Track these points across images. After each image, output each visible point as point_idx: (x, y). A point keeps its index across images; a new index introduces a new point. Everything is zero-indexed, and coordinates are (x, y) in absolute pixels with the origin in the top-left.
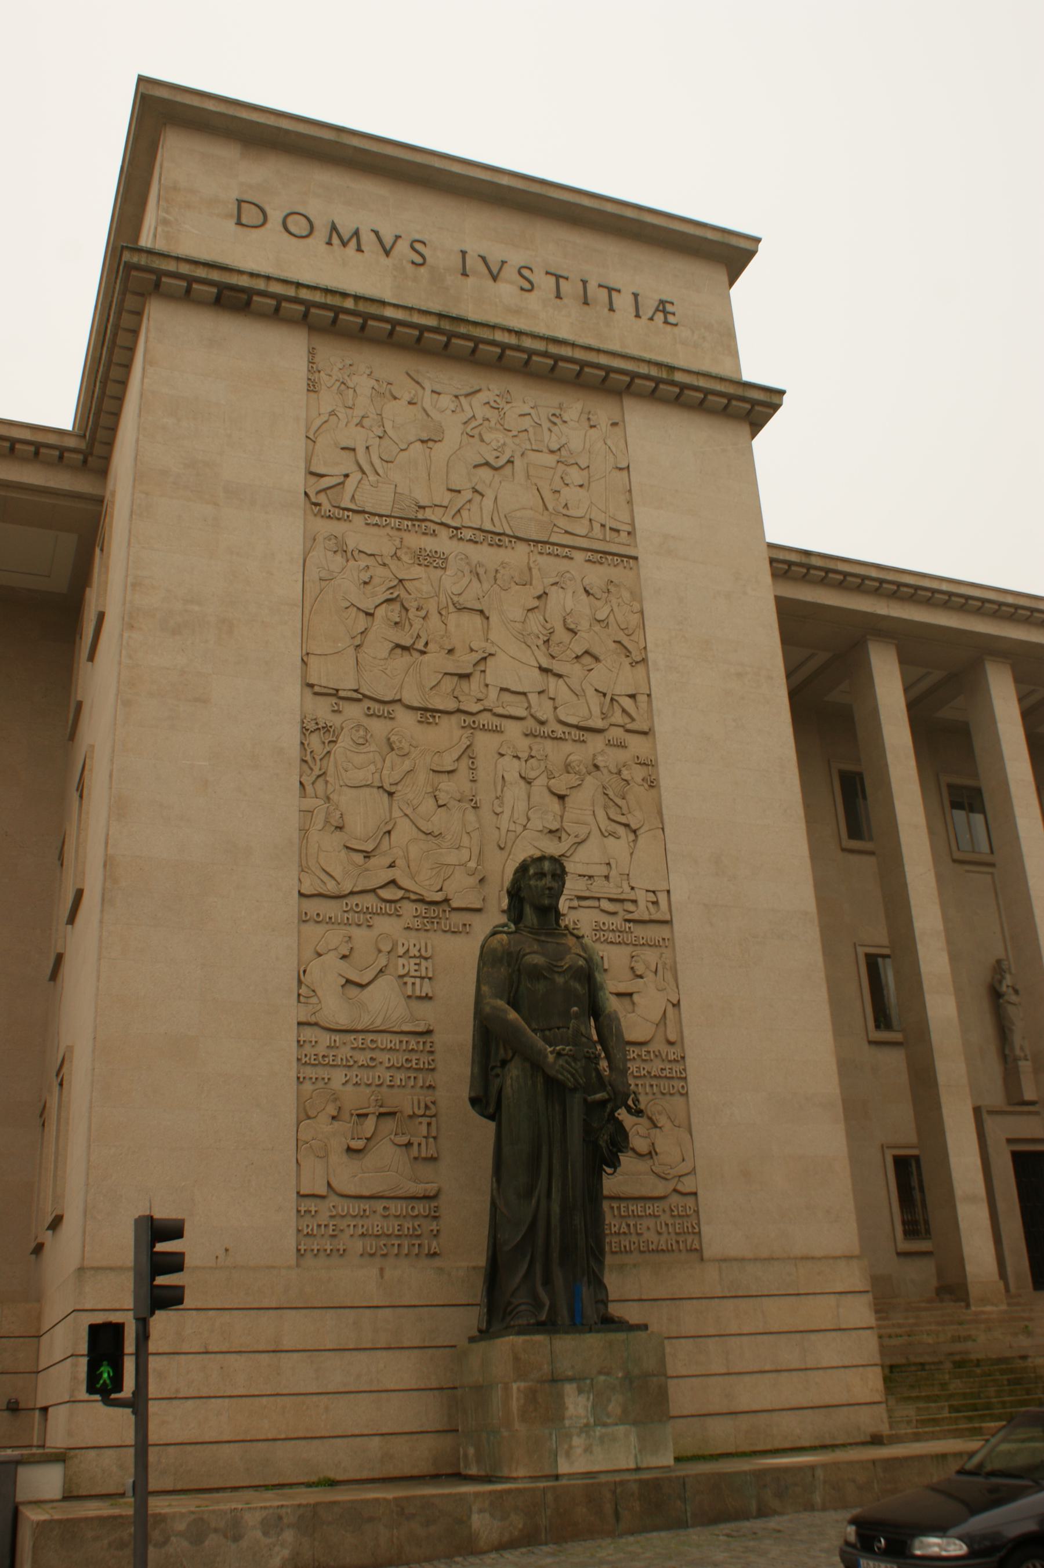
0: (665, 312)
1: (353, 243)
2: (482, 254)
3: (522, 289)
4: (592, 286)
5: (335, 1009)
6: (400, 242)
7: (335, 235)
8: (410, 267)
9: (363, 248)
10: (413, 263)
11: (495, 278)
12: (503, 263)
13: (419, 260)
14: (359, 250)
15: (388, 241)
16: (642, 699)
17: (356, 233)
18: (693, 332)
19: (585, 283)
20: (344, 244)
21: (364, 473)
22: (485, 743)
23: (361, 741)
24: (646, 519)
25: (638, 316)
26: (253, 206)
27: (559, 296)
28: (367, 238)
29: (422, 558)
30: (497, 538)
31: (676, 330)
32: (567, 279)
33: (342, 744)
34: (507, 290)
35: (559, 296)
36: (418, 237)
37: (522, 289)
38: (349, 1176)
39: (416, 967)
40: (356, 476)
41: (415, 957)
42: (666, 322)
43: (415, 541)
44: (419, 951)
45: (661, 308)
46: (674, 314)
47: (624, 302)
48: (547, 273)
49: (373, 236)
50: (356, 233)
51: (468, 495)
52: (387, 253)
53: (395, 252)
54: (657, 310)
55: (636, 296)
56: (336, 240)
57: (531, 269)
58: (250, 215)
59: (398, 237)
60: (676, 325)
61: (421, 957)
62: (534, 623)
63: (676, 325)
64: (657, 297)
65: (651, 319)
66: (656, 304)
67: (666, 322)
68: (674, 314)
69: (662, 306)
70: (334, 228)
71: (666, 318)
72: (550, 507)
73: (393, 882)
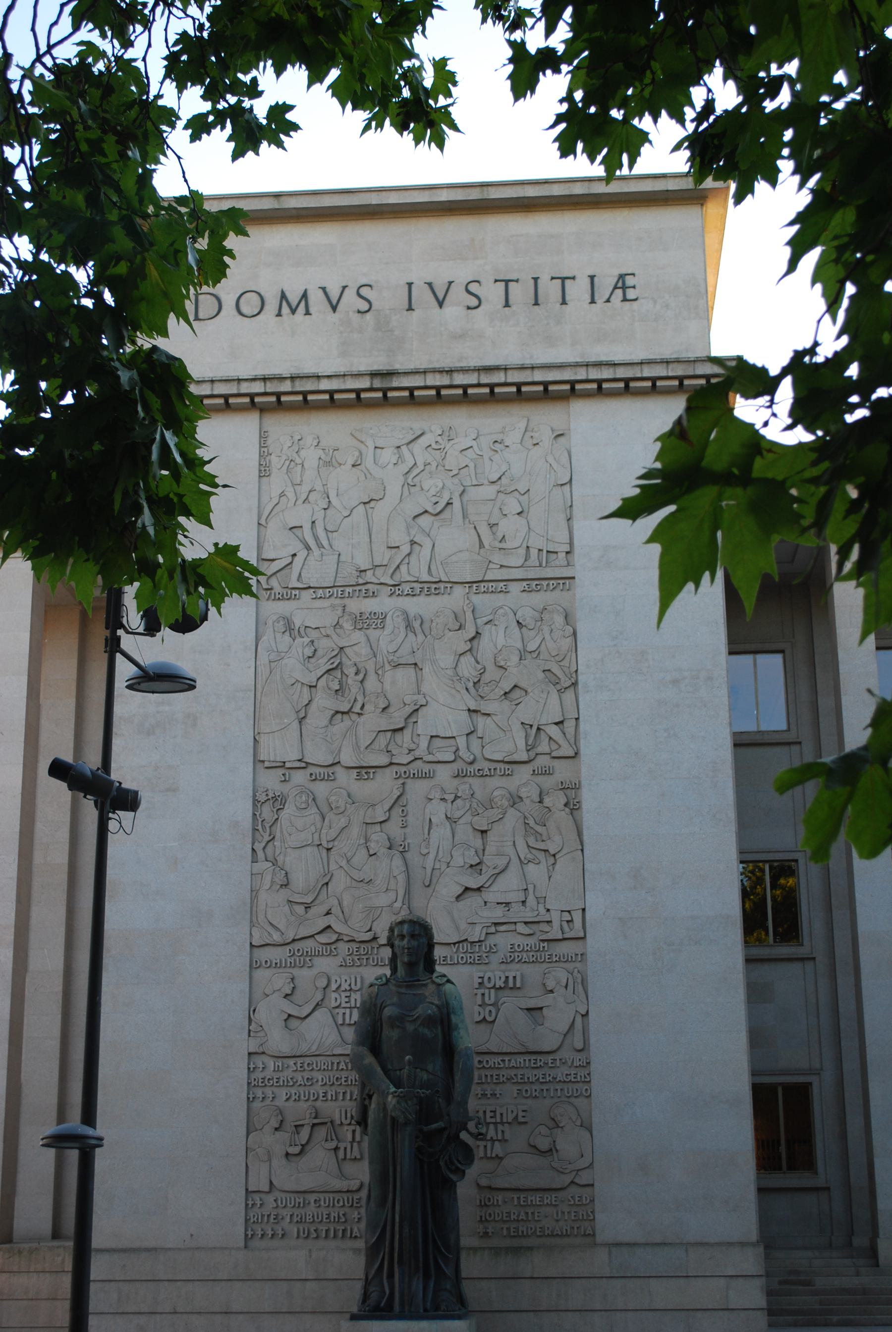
16: (569, 725)
17: (305, 296)
20: (293, 311)
21: (308, 548)
22: (417, 789)
28: (316, 297)
29: (362, 622)
30: (434, 587)
43: (356, 605)
50: (305, 296)
51: (406, 549)
52: (334, 308)
56: (285, 310)
62: (467, 667)
70: (283, 296)
72: (486, 543)
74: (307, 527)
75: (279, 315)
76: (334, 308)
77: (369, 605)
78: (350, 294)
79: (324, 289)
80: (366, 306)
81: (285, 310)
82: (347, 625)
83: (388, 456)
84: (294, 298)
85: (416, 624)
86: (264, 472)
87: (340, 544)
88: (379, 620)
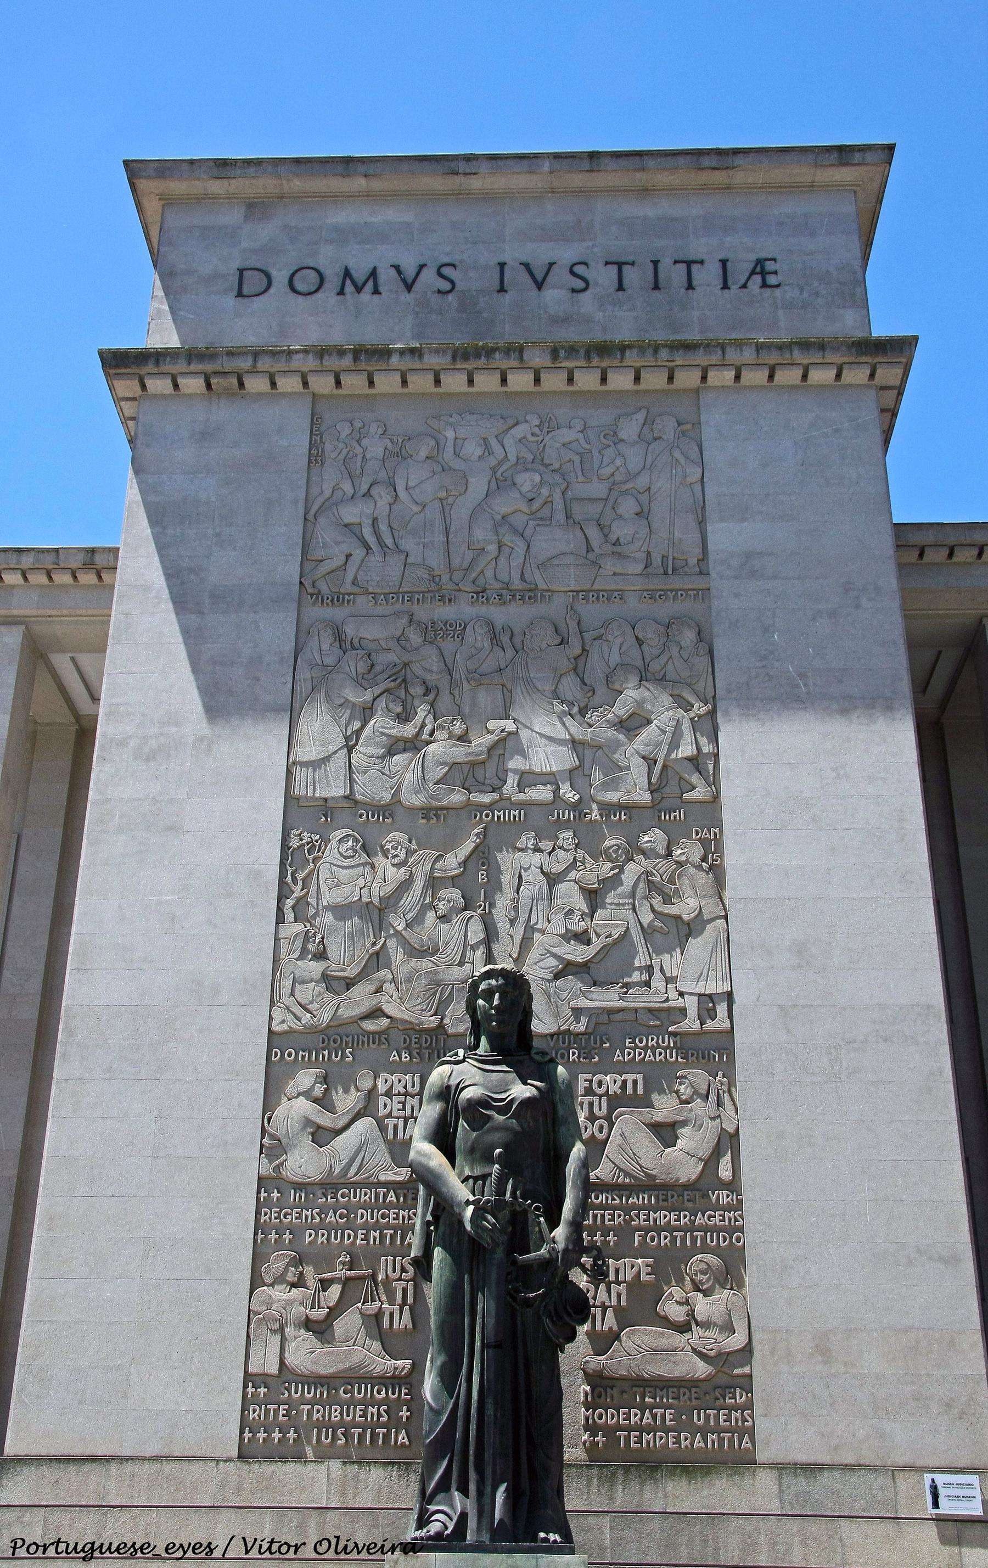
0: (763, 273)
1: (370, 286)
2: (524, 260)
3: (573, 291)
4: (666, 264)
5: (304, 1162)
6: (425, 271)
7: (348, 282)
8: (435, 300)
9: (381, 289)
10: (439, 292)
11: (540, 286)
12: (551, 265)
13: (448, 286)
14: (376, 291)
15: (410, 273)
17: (373, 274)
18: (802, 290)
19: (655, 263)
20: (359, 289)
21: (368, 548)
23: (350, 853)
24: (725, 537)
25: (725, 286)
26: (256, 272)
27: (621, 288)
28: (387, 276)
31: (778, 292)
32: (633, 264)
33: (328, 859)
34: (554, 296)
35: (621, 288)
36: (446, 260)
37: (573, 291)
38: (304, 1353)
39: (400, 1106)
40: (359, 553)
41: (399, 1094)
42: (764, 285)
44: (405, 1087)
45: (758, 269)
46: (776, 273)
47: (707, 275)
48: (607, 263)
49: (393, 272)
50: (373, 274)
52: (409, 287)
53: (417, 287)
54: (753, 273)
55: (724, 263)
56: (349, 288)
57: (586, 264)
58: (253, 282)
59: (422, 267)
60: (778, 286)
61: (406, 1094)
63: (778, 286)
64: (753, 257)
65: (744, 286)
66: (753, 265)
67: (764, 285)
68: (776, 273)
69: (760, 268)
70: (347, 273)
71: (764, 280)
72: (595, 544)
73: (376, 1013)
74: (367, 522)
75: (341, 292)
76: (409, 287)
77: (445, 612)
78: (428, 276)
79: (397, 268)
80: (446, 286)
81: (349, 288)
82: (415, 638)
83: (472, 449)
84: (360, 276)
85: (505, 639)
86: (315, 457)
87: (408, 544)
88: (459, 629)
